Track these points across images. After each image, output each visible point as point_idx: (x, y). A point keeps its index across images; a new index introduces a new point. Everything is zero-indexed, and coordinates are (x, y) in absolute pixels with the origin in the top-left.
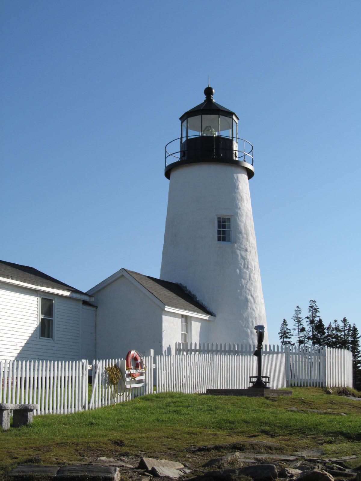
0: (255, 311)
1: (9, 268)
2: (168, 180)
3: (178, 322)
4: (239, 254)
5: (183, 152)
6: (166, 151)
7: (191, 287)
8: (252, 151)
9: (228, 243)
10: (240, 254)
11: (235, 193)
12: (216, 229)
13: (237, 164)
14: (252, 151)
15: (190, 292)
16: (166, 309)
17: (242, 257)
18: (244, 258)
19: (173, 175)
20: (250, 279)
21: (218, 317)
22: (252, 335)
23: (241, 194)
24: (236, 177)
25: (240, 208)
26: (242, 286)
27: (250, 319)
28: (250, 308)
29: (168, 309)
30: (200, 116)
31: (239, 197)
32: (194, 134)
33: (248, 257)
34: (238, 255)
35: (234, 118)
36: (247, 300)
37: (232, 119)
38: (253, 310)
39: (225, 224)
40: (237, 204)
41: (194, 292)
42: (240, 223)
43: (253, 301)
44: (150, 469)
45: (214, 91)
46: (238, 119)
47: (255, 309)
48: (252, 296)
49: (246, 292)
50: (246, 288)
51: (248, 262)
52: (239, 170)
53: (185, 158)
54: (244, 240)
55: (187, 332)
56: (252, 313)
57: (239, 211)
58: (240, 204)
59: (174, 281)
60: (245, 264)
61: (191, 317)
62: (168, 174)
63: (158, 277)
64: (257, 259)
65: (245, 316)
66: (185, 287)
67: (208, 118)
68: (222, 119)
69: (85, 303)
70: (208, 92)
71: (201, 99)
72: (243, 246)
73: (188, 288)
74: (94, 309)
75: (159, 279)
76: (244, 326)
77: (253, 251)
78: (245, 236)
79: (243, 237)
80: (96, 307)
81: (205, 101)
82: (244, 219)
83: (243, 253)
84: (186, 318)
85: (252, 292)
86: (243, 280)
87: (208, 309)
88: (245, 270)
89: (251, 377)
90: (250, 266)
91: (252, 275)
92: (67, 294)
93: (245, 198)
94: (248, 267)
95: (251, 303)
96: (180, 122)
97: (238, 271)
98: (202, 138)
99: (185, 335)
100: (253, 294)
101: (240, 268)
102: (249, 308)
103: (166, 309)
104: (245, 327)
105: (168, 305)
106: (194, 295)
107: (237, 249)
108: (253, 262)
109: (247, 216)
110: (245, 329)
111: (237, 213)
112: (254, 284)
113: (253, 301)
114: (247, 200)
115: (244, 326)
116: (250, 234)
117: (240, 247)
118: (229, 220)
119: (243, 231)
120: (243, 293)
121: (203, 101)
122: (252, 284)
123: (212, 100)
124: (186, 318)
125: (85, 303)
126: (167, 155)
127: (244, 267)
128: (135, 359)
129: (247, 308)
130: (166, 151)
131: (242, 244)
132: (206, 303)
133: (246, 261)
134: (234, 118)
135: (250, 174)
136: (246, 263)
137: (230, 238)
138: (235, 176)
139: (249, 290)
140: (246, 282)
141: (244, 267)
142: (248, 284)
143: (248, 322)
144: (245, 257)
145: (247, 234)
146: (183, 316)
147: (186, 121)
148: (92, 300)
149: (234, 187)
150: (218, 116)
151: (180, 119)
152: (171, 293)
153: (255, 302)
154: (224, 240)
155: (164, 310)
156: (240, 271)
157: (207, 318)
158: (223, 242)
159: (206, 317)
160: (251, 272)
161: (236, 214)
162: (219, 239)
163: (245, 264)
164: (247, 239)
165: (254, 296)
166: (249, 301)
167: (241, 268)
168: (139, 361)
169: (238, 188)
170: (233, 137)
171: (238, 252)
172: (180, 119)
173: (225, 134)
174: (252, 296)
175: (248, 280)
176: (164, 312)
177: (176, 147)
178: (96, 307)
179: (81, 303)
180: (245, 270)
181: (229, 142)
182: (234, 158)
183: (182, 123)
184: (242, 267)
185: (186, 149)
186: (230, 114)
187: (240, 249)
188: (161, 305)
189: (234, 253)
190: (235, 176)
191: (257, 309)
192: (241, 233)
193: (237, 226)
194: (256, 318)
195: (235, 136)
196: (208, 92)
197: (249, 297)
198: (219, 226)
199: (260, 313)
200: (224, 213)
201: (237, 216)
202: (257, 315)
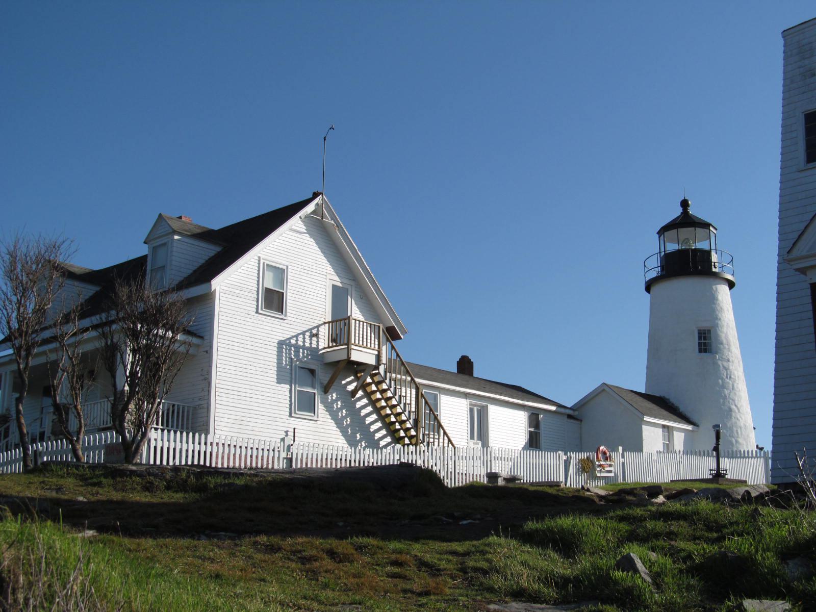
0: (739, 420)
1: (498, 386)
2: (648, 294)
4: (721, 365)
5: (662, 267)
6: (645, 265)
7: (674, 400)
8: (732, 260)
9: (710, 354)
10: (722, 364)
11: (714, 304)
12: (697, 340)
13: (715, 275)
14: (732, 260)
15: (673, 404)
16: (645, 419)
17: (724, 367)
18: (726, 369)
19: (654, 289)
20: (733, 389)
21: (700, 426)
22: (737, 445)
23: (721, 305)
24: (714, 289)
25: (720, 319)
26: (726, 396)
27: (735, 429)
28: (735, 418)
29: (646, 419)
30: (676, 230)
31: (719, 309)
32: (672, 247)
33: (731, 367)
34: (719, 366)
35: (711, 228)
36: (730, 410)
37: (708, 230)
38: (738, 419)
39: (706, 336)
40: (717, 316)
42: (720, 334)
43: (737, 411)
44: (586, 489)
45: (690, 202)
46: (716, 229)
47: (740, 419)
48: (736, 406)
49: (729, 402)
50: (729, 398)
51: (731, 372)
52: (718, 281)
53: (664, 273)
54: (725, 350)
55: (669, 441)
56: (736, 423)
57: (719, 322)
58: (720, 315)
59: (658, 395)
60: (727, 374)
61: (673, 427)
62: (648, 289)
63: (643, 391)
64: (741, 369)
65: (729, 426)
66: (669, 400)
67: (684, 232)
68: (699, 231)
69: (570, 417)
70: (685, 204)
71: (678, 211)
72: (724, 357)
73: (671, 400)
74: (579, 422)
75: (644, 392)
76: (728, 435)
77: (736, 361)
78: (726, 346)
79: (725, 348)
80: (581, 421)
81: (682, 213)
82: (725, 330)
83: (725, 364)
85: (736, 402)
86: (725, 390)
87: (691, 420)
88: (728, 380)
89: (711, 470)
90: (732, 377)
91: (735, 385)
92: (553, 408)
93: (725, 308)
94: (730, 377)
95: (735, 412)
96: (657, 236)
97: (720, 381)
98: (679, 252)
99: (668, 444)
100: (737, 404)
101: (722, 379)
102: (733, 418)
103: (645, 419)
104: (730, 436)
105: (646, 415)
106: (677, 407)
107: (719, 359)
108: (736, 373)
109: (728, 326)
110: (730, 438)
111: (718, 324)
112: (737, 393)
113: (737, 411)
114: (728, 310)
115: (728, 435)
116: (732, 344)
117: (722, 358)
118: (709, 331)
119: (725, 341)
120: (727, 403)
121: (680, 214)
122: (735, 394)
123: (688, 212)
125: (570, 417)
126: (646, 270)
127: (727, 378)
128: (604, 453)
129: (731, 418)
130: (645, 265)
131: (723, 355)
132: (688, 414)
133: (728, 371)
134: (711, 228)
135: (731, 285)
136: (729, 373)
137: (711, 349)
138: (714, 287)
139: (733, 400)
140: (729, 391)
141: (727, 378)
142: (731, 394)
143: (733, 432)
144: (727, 367)
145: (729, 344)
146: (664, 426)
147: (663, 236)
148: (576, 413)
149: (712, 299)
150: (694, 228)
151: (658, 233)
152: (654, 405)
153: (739, 412)
154: (705, 351)
155: (643, 420)
156: (723, 382)
157: (691, 429)
158: (705, 354)
159: (689, 427)
160: (734, 382)
161: (717, 325)
162: (700, 351)
163: (727, 374)
164: (729, 350)
165: (739, 406)
166: (733, 410)
167: (723, 378)
168: (608, 455)
169: (717, 300)
170: (711, 249)
171: (720, 363)
172: (658, 233)
173: (702, 245)
174: (736, 406)
175: (731, 389)
176: (643, 422)
177: (655, 262)
178: (581, 421)
179: (566, 416)
180: (728, 380)
181: (708, 253)
182: (714, 270)
183: (659, 237)
184: (725, 377)
185: (664, 264)
186: (706, 225)
187: (722, 359)
188: (640, 414)
189: (715, 364)
190: (714, 287)
191: (742, 419)
192: (722, 343)
193: (717, 336)
194: (741, 428)
195: (713, 247)
196: (685, 204)
197: (733, 407)
198: (700, 338)
199: (745, 422)
200: (704, 325)
201: (718, 327)
202: (742, 425)
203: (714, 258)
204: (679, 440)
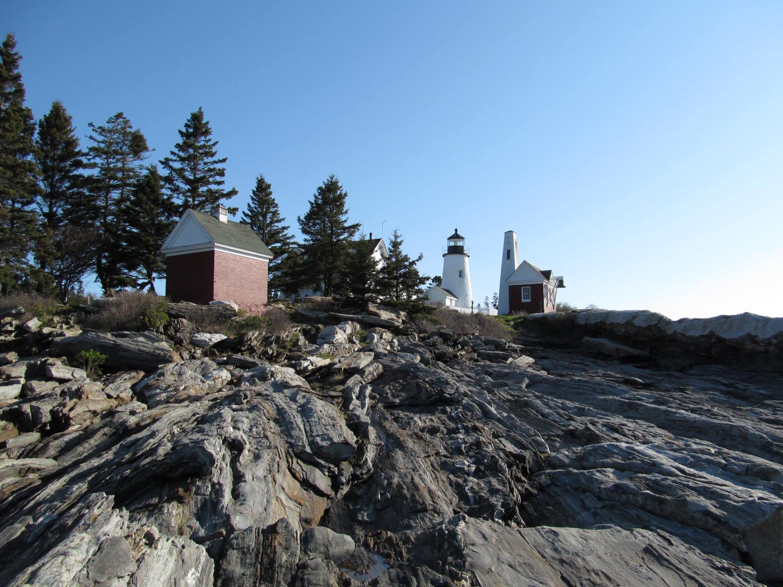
3: (449, 300)
7: (451, 290)
13: (465, 254)
32: (452, 244)
41: (452, 292)
70: (456, 230)
71: (454, 232)
84: (451, 299)
98: (455, 246)
124: (451, 299)
132: (456, 295)
135: (468, 256)
149: (464, 261)
159: (456, 299)
161: (464, 270)
181: (463, 247)
186: (463, 238)
189: (464, 281)
196: (456, 230)
200: (461, 269)
203: (465, 248)
204: (454, 302)
